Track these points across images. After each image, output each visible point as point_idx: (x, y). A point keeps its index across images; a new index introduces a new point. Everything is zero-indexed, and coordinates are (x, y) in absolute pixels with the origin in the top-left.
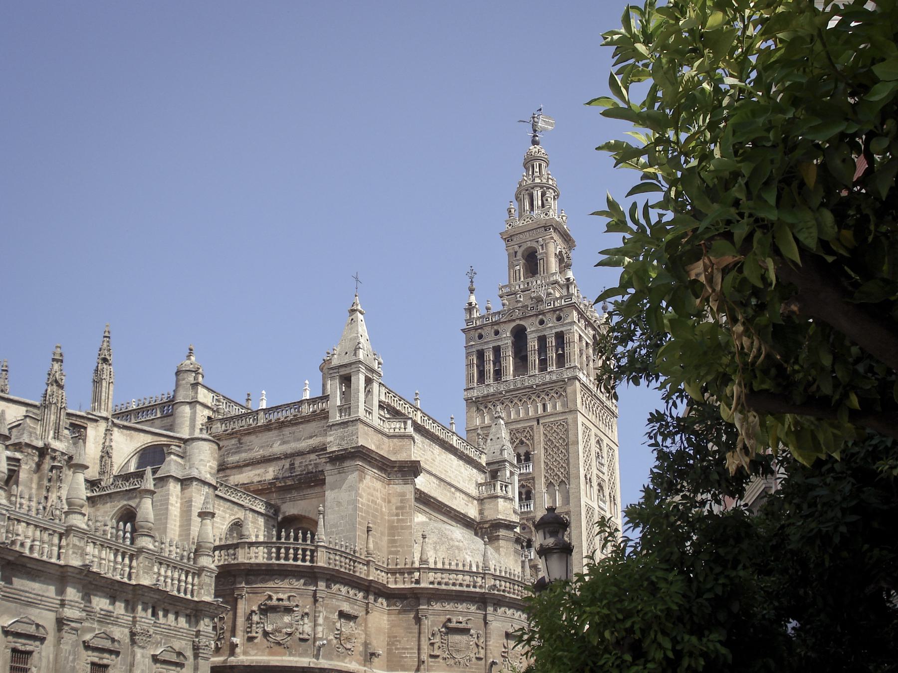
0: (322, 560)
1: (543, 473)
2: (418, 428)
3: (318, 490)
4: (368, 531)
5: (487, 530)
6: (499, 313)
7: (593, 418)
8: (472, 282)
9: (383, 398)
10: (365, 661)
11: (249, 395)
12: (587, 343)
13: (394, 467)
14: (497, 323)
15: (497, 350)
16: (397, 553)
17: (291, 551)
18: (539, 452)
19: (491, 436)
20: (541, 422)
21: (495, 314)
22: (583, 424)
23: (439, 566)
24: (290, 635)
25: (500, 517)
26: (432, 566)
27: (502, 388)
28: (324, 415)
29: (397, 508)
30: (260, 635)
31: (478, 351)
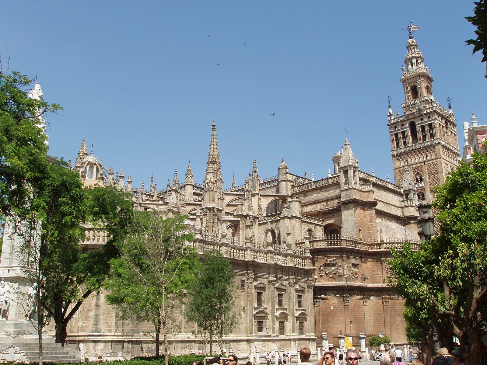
0: (344, 245)
1: (429, 186)
2: (375, 185)
3: (338, 214)
4: (360, 231)
5: (404, 221)
6: (403, 116)
7: (449, 159)
8: (389, 103)
9: (361, 176)
10: (363, 281)
11: (305, 173)
12: (443, 126)
13: (367, 204)
14: (402, 121)
15: (403, 133)
16: (371, 237)
17: (333, 242)
18: (426, 177)
19: (404, 179)
20: (426, 163)
21: (401, 117)
22: (444, 163)
23: (388, 242)
24: (335, 274)
25: (411, 215)
26: (385, 242)
27: (407, 149)
28: (338, 184)
29: (369, 220)
30: (324, 275)
31: (395, 133)
